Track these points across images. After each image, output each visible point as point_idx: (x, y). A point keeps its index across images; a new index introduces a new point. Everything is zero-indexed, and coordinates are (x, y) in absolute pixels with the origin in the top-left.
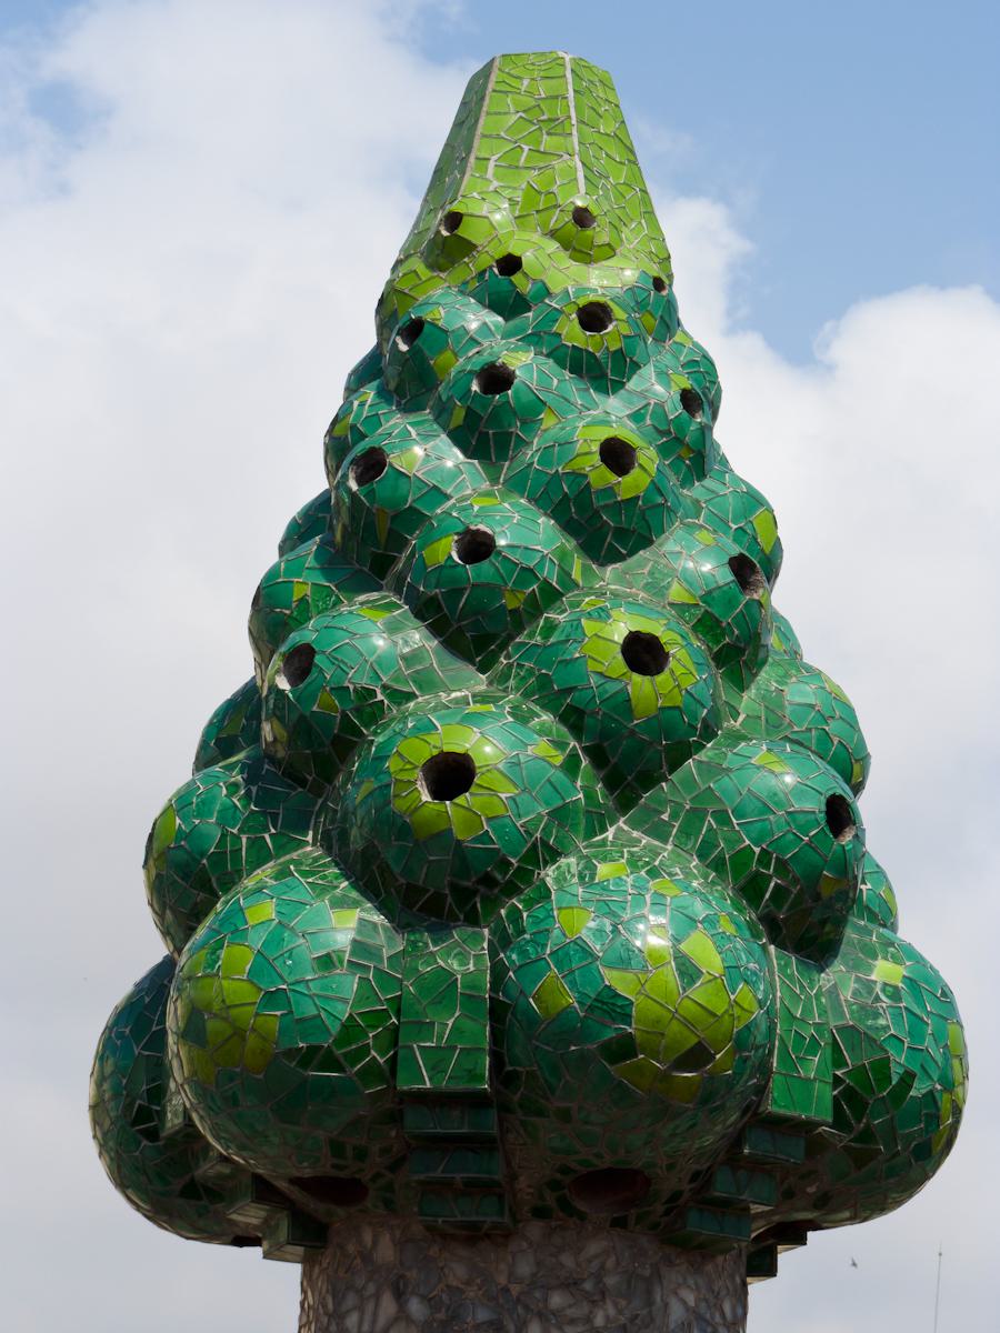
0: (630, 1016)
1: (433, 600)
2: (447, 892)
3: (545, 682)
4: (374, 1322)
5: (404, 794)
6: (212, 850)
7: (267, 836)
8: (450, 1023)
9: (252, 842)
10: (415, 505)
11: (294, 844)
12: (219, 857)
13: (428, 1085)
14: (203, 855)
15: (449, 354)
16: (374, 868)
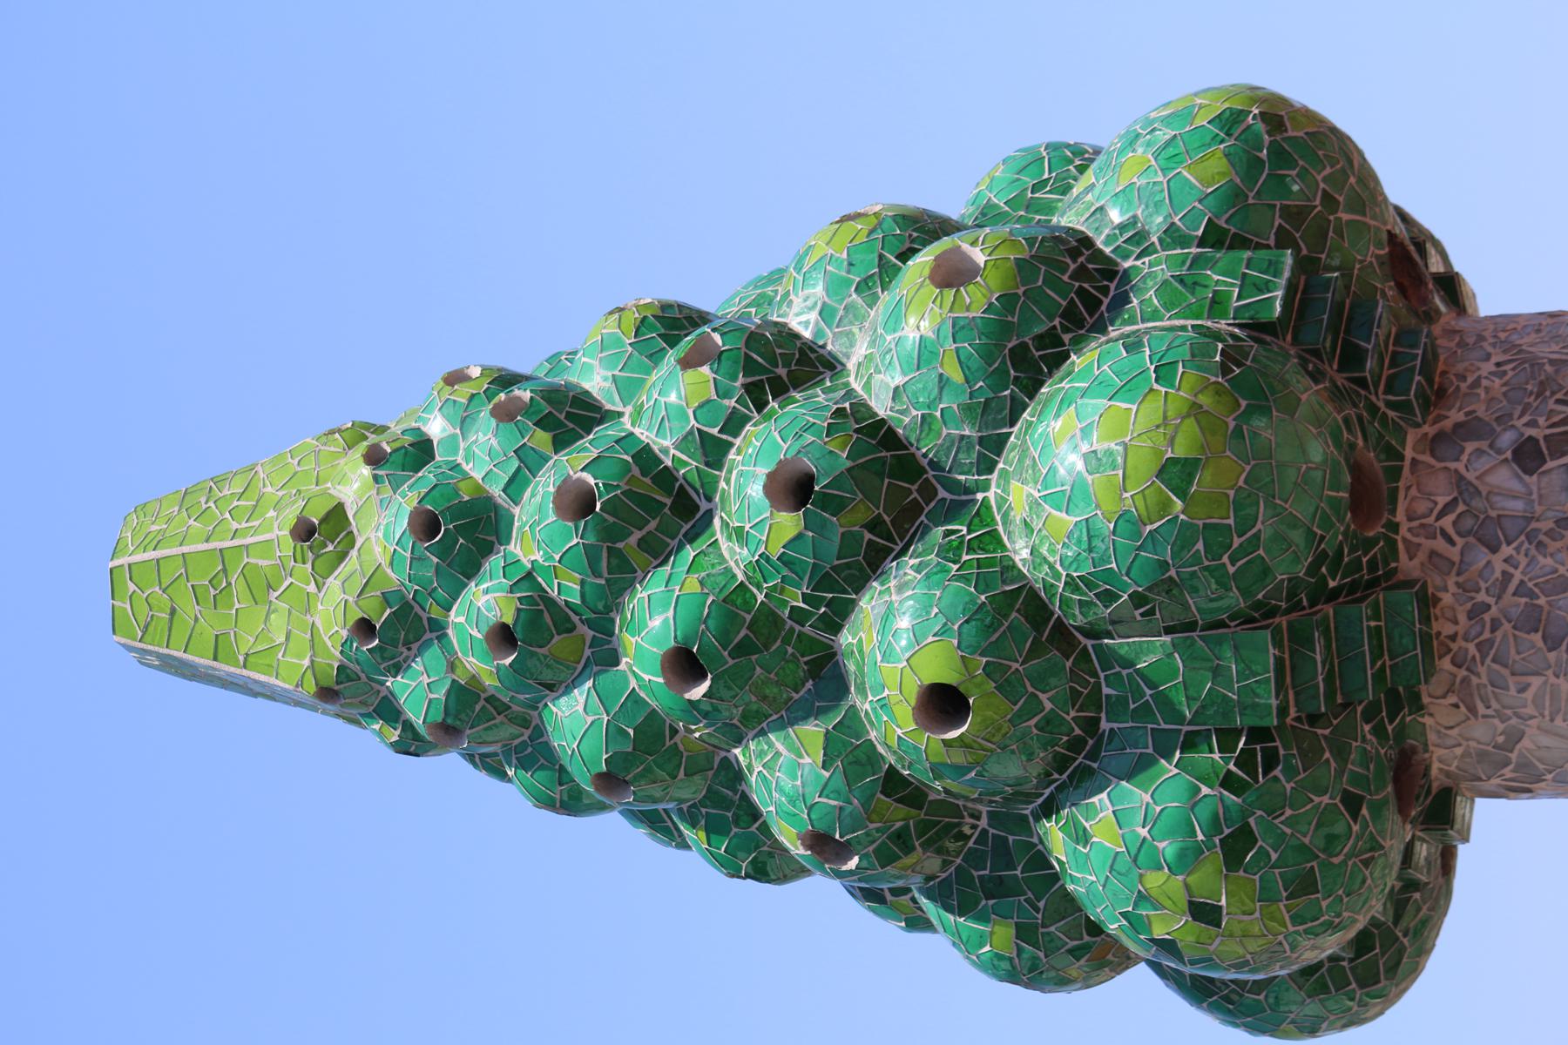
0: (1242, 111)
1: (748, 388)
2: (1077, 284)
3: (863, 286)
4: (1515, 498)
5: (968, 300)
6: (973, 590)
7: (969, 537)
8: (1216, 277)
9: (970, 550)
10: (633, 452)
11: (983, 510)
12: (982, 583)
13: (1280, 293)
14: (973, 601)
15: (462, 485)
16: (1037, 354)
